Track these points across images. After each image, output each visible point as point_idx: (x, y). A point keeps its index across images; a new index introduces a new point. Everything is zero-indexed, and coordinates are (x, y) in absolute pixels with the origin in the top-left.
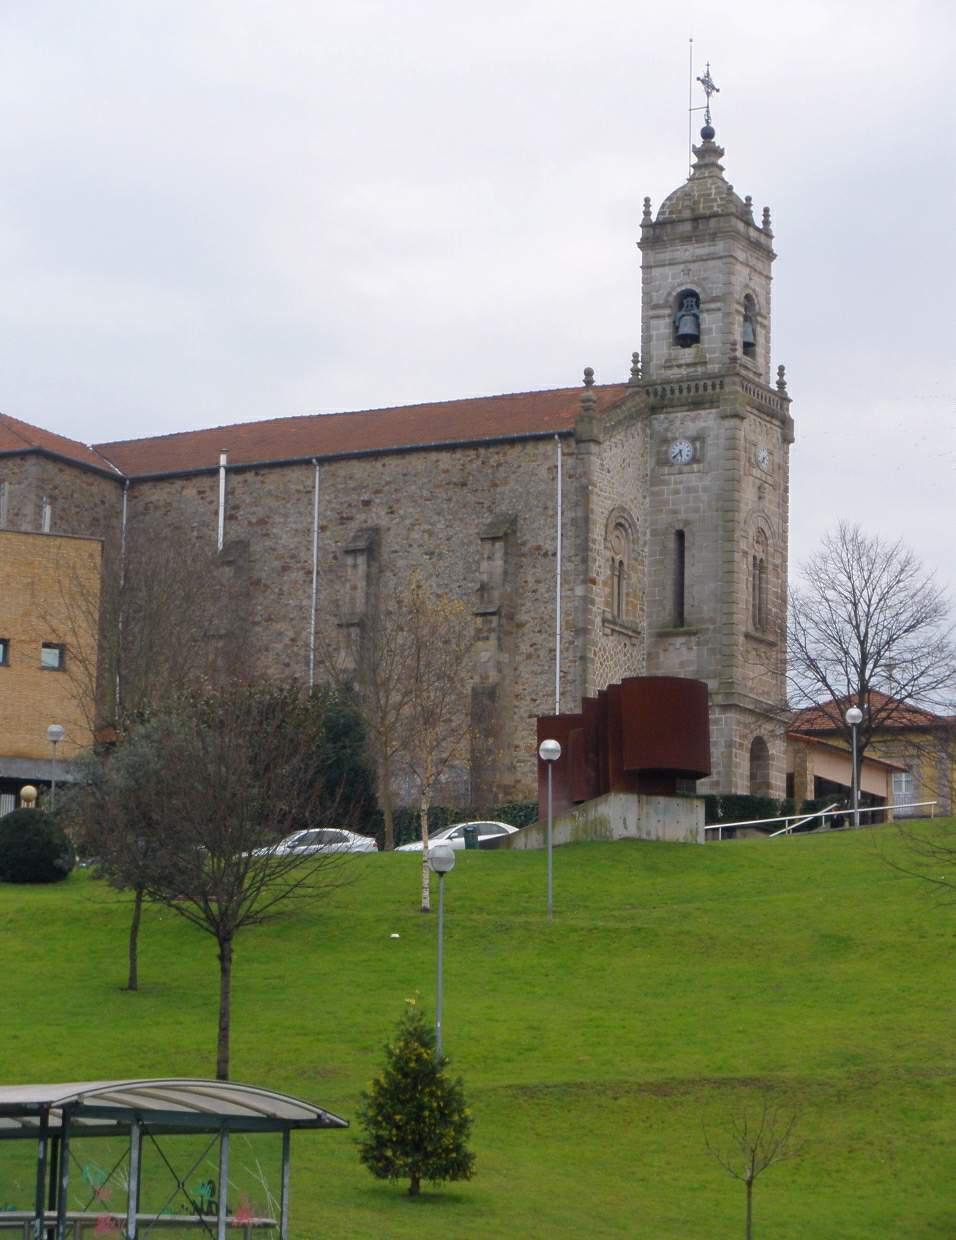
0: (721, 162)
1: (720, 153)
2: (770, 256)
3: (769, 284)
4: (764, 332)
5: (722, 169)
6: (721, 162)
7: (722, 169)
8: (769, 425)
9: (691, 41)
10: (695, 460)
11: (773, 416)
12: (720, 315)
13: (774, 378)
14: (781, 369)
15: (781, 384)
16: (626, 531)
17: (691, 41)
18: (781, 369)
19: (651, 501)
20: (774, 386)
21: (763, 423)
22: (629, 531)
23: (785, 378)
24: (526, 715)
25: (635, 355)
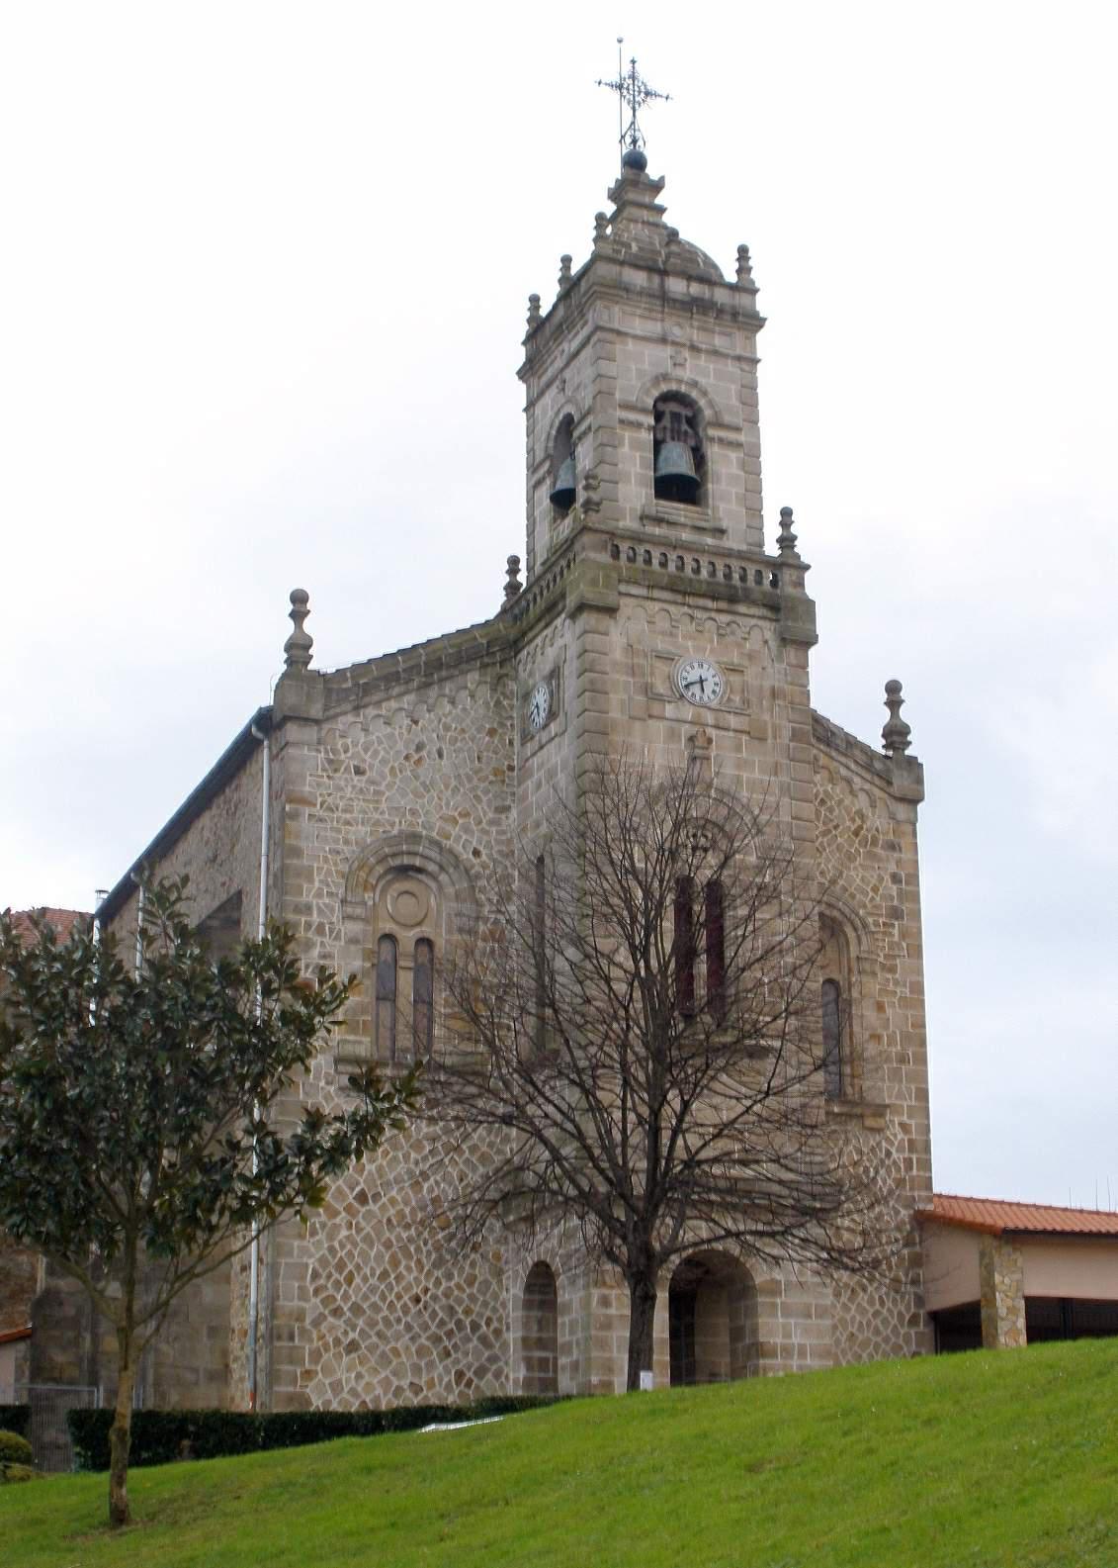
0: (659, 200)
1: (657, 187)
2: (755, 322)
3: (753, 373)
4: (734, 456)
5: (661, 210)
6: (659, 200)
7: (661, 210)
8: (724, 618)
9: (620, 41)
10: (552, 715)
11: (733, 599)
12: (591, 436)
13: (772, 531)
14: (786, 514)
15: (787, 542)
16: (435, 878)
17: (620, 41)
18: (786, 514)
19: (519, 814)
20: (772, 549)
21: (698, 614)
22: (443, 877)
23: (794, 529)
24: (239, 1268)
25: (514, 562)
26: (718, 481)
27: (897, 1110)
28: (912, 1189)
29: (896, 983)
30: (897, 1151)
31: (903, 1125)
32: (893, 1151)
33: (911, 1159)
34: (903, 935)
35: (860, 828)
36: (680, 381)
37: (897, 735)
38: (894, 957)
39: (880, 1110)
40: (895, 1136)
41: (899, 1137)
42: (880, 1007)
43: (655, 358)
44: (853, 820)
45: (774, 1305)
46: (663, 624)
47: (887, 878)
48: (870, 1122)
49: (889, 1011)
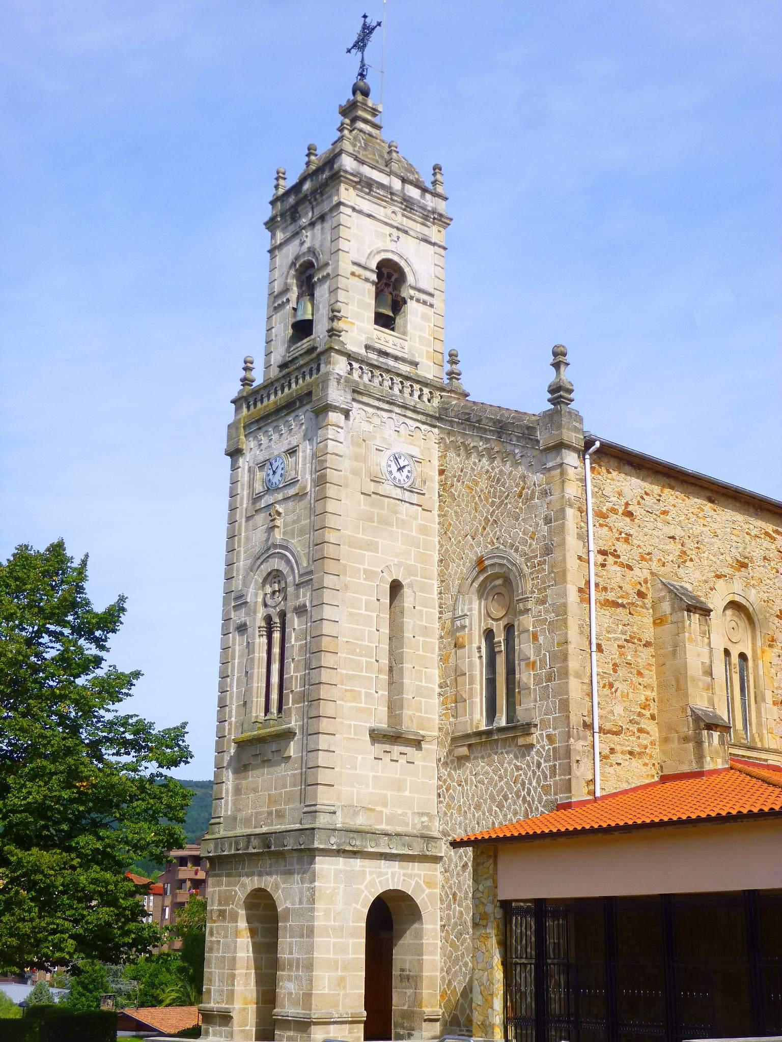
26: (319, 309)
27: (544, 724)
28: (556, 794)
29: (547, 611)
30: (545, 761)
31: (549, 737)
32: (542, 761)
33: (555, 766)
34: (552, 566)
35: (523, 488)
36: (304, 254)
37: (559, 394)
38: (545, 589)
39: (527, 728)
40: (543, 747)
41: (547, 748)
42: (535, 637)
43: (291, 250)
44: (517, 485)
45: (286, 927)
46: (264, 440)
47: (541, 522)
48: (521, 741)
49: (541, 639)
